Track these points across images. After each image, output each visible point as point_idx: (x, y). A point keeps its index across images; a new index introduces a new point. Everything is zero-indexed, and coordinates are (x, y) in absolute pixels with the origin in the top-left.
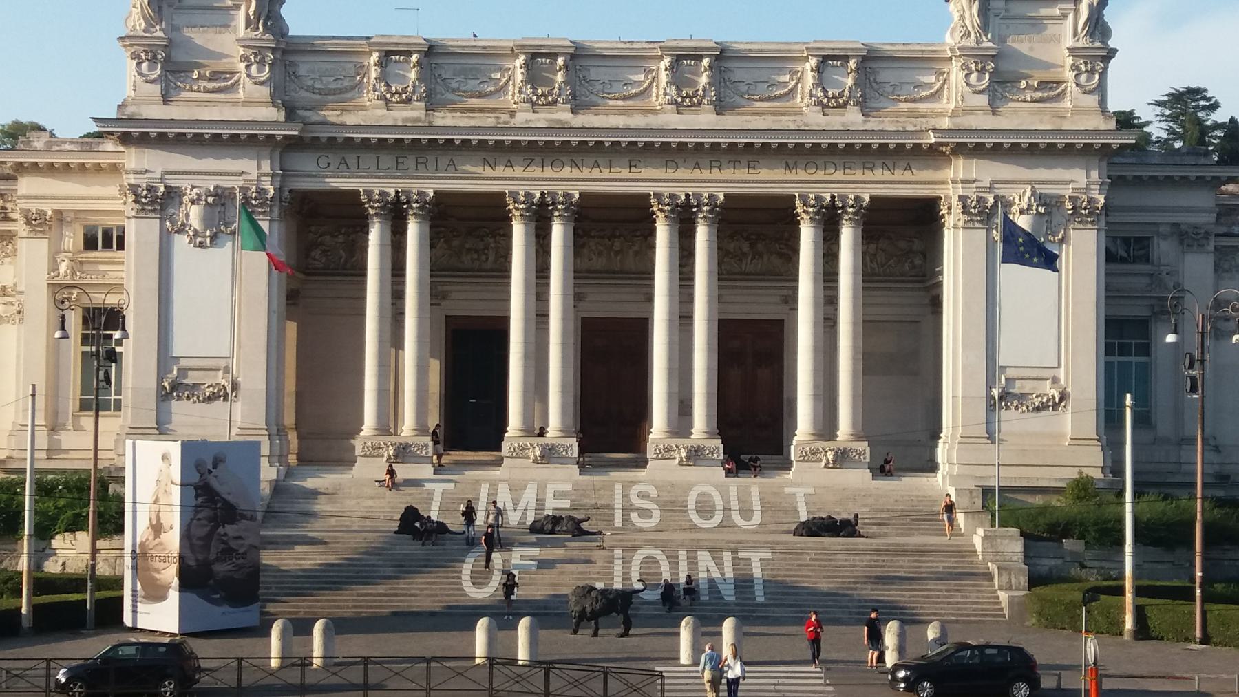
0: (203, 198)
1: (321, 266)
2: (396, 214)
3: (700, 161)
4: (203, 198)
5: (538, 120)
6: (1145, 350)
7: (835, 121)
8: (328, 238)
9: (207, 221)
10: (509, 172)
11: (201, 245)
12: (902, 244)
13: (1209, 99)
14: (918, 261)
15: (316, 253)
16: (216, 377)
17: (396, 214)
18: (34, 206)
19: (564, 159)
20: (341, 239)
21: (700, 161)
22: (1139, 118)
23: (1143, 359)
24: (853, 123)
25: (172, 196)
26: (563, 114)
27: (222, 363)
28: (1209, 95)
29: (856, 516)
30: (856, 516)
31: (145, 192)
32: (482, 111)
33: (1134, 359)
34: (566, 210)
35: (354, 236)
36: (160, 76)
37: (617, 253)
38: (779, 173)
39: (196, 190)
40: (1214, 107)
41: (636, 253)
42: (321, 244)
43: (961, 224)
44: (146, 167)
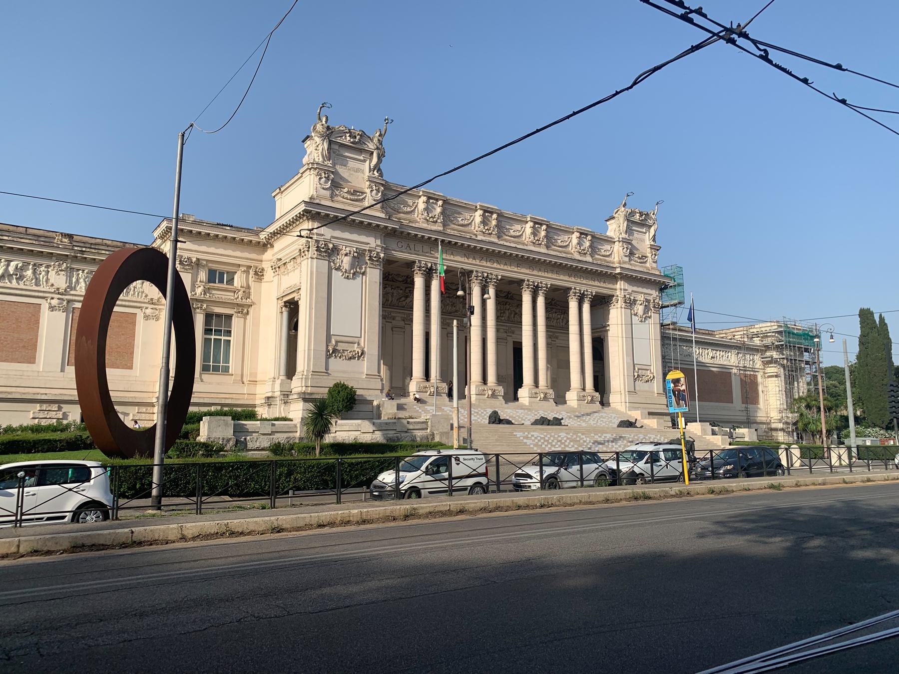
0: (352, 253)
2: (429, 274)
3: (541, 268)
4: (352, 253)
9: (352, 266)
10: (474, 262)
11: (347, 278)
16: (354, 347)
17: (429, 274)
18: (186, 255)
19: (494, 259)
21: (541, 268)
25: (335, 250)
27: (356, 340)
29: (636, 420)
30: (636, 420)
31: (323, 246)
34: (495, 282)
36: (330, 187)
38: (566, 278)
39: (348, 249)
43: (623, 306)
44: (322, 233)
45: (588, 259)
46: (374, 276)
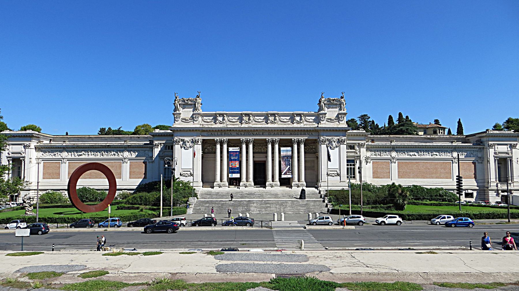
1: (207, 152)
5: (246, 126)
6: (354, 165)
7: (299, 126)
8: (208, 147)
12: (311, 147)
13: (368, 116)
14: (314, 150)
15: (206, 150)
20: (211, 147)
22: (355, 120)
23: (354, 167)
24: (302, 126)
26: (250, 125)
28: (368, 116)
32: (236, 124)
33: (352, 167)
35: (213, 147)
37: (260, 149)
40: (369, 118)
41: (264, 149)
42: (207, 148)
45: (302, 125)
46: (198, 148)
